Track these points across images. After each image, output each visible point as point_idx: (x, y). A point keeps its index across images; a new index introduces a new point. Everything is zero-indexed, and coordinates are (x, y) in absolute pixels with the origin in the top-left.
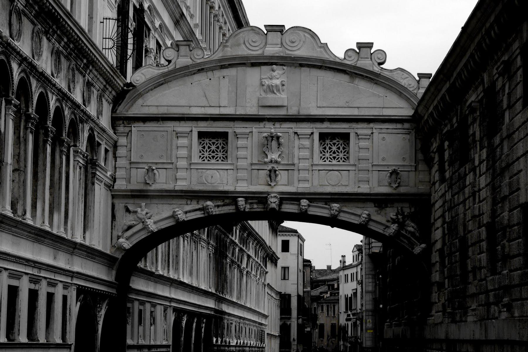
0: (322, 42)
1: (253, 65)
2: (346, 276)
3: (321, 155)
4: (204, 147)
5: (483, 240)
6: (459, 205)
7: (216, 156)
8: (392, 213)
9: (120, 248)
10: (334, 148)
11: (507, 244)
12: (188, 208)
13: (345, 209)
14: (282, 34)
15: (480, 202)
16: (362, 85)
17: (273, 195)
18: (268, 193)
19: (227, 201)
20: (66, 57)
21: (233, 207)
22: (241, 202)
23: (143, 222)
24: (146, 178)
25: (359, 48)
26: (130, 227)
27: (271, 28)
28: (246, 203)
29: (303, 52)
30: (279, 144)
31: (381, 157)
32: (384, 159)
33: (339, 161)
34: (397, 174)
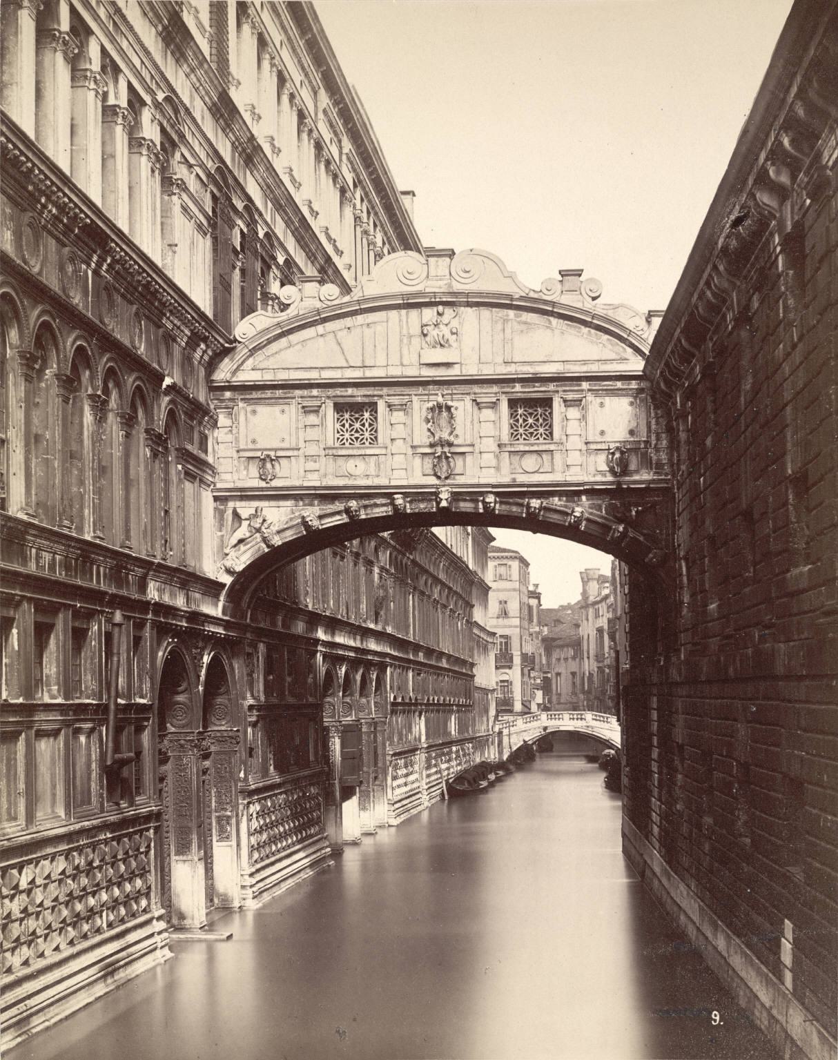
0: (509, 269)
3: (512, 431)
4: (343, 426)
7: (361, 437)
9: (229, 571)
10: (530, 421)
14: (452, 260)
17: (443, 489)
18: (437, 487)
20: (123, 296)
21: (390, 508)
22: (399, 501)
25: (562, 276)
26: (241, 541)
28: (405, 501)
31: (598, 432)
32: (602, 433)
33: (538, 439)
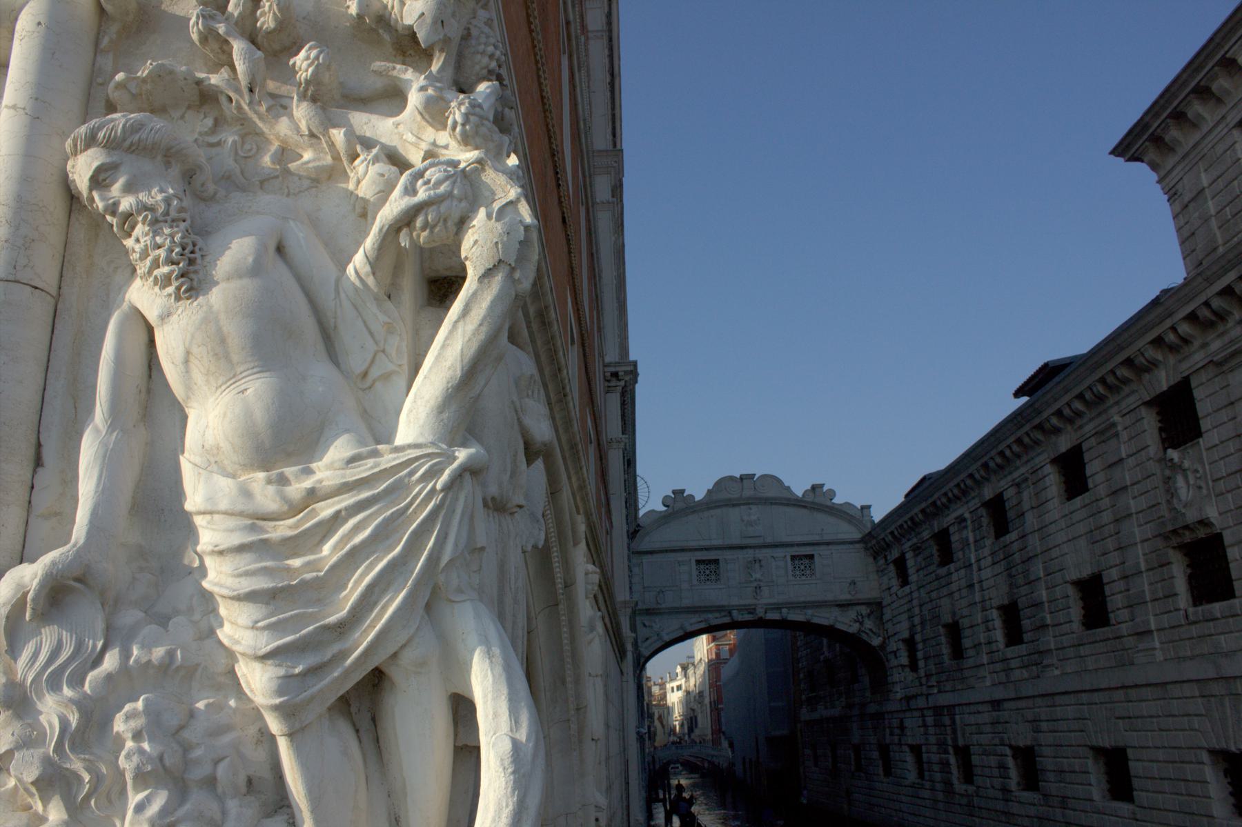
0: (786, 484)
1: (734, 505)
2: (673, 688)
5: (993, 620)
6: (940, 598)
8: (852, 614)
10: (802, 567)
11: (1048, 616)
12: (693, 621)
13: (816, 614)
15: (983, 590)
16: (820, 516)
18: (755, 605)
19: (723, 614)
22: (735, 613)
23: (658, 635)
24: (658, 599)
27: (742, 478)
29: (771, 493)
30: (761, 566)
34: (855, 583)
